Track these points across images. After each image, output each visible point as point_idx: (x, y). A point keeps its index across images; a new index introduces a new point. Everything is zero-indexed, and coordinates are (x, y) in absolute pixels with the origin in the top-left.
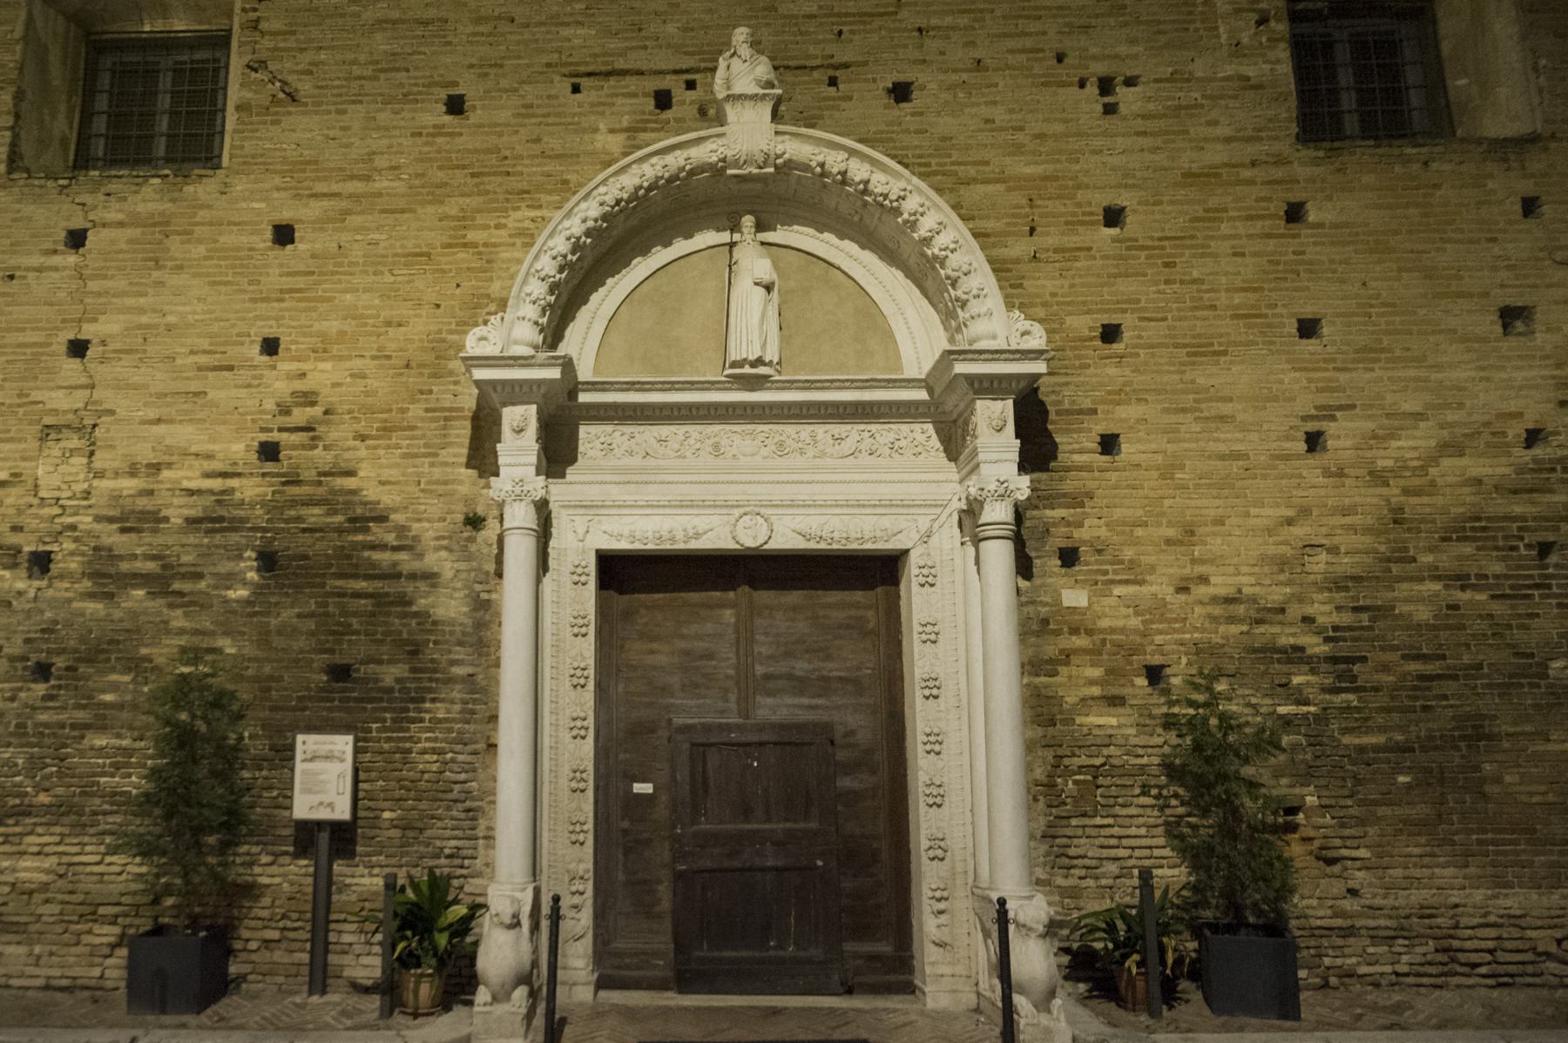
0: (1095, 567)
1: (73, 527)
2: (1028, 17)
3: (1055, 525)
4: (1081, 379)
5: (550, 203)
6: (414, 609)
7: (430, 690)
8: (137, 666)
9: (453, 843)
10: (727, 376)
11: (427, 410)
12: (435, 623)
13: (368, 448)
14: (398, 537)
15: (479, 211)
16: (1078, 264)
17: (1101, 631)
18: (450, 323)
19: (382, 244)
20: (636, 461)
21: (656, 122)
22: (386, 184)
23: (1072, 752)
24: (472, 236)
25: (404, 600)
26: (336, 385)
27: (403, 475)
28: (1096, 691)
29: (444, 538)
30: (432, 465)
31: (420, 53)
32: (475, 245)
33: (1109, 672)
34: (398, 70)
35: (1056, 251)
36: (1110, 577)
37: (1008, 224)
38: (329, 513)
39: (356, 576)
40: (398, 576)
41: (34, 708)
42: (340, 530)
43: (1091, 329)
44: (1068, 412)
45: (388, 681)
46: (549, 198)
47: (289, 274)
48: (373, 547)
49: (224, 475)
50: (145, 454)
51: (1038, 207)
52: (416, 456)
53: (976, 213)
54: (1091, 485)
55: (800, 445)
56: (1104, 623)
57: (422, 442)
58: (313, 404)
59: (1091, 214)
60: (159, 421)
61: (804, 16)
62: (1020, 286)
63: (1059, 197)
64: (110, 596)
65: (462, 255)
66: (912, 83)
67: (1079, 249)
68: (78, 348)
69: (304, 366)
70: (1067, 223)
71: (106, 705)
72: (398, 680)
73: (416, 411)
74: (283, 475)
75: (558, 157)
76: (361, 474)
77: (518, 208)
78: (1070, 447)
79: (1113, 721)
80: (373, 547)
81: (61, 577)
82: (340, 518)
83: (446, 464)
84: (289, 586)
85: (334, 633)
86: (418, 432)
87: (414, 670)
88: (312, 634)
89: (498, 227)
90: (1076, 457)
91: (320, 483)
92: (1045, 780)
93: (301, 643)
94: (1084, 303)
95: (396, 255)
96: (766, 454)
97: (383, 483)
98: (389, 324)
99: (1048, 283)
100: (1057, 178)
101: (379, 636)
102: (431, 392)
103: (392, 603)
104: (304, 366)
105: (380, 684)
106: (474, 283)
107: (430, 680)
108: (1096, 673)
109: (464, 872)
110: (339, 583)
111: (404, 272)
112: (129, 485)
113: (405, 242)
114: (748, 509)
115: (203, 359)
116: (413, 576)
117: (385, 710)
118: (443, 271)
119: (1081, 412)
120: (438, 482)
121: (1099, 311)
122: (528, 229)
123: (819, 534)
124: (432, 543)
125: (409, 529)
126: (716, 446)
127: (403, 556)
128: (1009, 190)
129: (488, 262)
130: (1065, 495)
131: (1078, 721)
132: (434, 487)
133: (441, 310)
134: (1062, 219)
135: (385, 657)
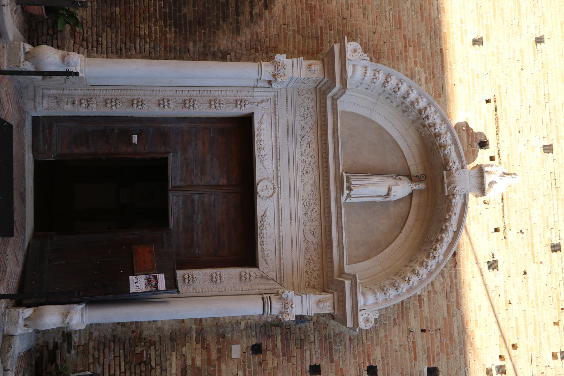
0: (252, 362)
2: (535, 328)
3: (273, 341)
4: (348, 355)
5: (429, 88)
6: (221, 22)
7: (181, 30)
9: (104, 42)
10: (342, 174)
12: (214, 32)
16: (407, 353)
17: (219, 365)
18: (365, 39)
19: (405, 5)
20: (299, 132)
21: (473, 141)
23: (158, 350)
24: (411, 49)
25: (225, 18)
27: (288, 16)
28: (189, 362)
29: (257, 37)
30: (294, 31)
31: (504, 22)
32: (406, 51)
33: (199, 369)
34: (495, 11)
35: (414, 342)
36: (247, 369)
37: (426, 318)
40: (238, 15)
43: (374, 360)
44: (331, 349)
45: (185, 10)
46: (431, 88)
51: (436, 334)
52: (298, 23)
53: (432, 302)
54: (294, 360)
55: (309, 213)
56: (223, 367)
57: (305, 25)
59: (434, 360)
61: (530, 214)
62: (395, 324)
63: (442, 345)
65: (400, 45)
66: (498, 270)
67: (415, 354)
70: (428, 348)
72: (185, 14)
77: (425, 72)
78: (313, 349)
79: (174, 371)
83: (294, 38)
86: (310, 24)
87: (190, 22)
89: (415, 62)
90: (308, 352)
92: (143, 337)
94: (387, 357)
95: (399, 11)
96: (304, 196)
98: (364, 9)
99: (397, 339)
100: (451, 343)
101: (207, 5)
102: (330, 30)
105: (183, 6)
106: (387, 51)
107: (186, 31)
108: (198, 363)
109: (90, 48)
111: (391, 16)
113: (406, 16)
114: (276, 187)
116: (238, 22)
117: (170, 8)
118: (392, 36)
119: (331, 355)
120: (285, 34)
121: (383, 364)
122: (415, 77)
123: (265, 223)
124: (254, 31)
125: (261, 19)
126: (308, 172)
127: (248, 17)
128: (445, 319)
129: (398, 58)
130: (288, 347)
131: (174, 354)
132: (283, 32)
133: (372, 35)
134: (430, 345)
135: (196, 8)
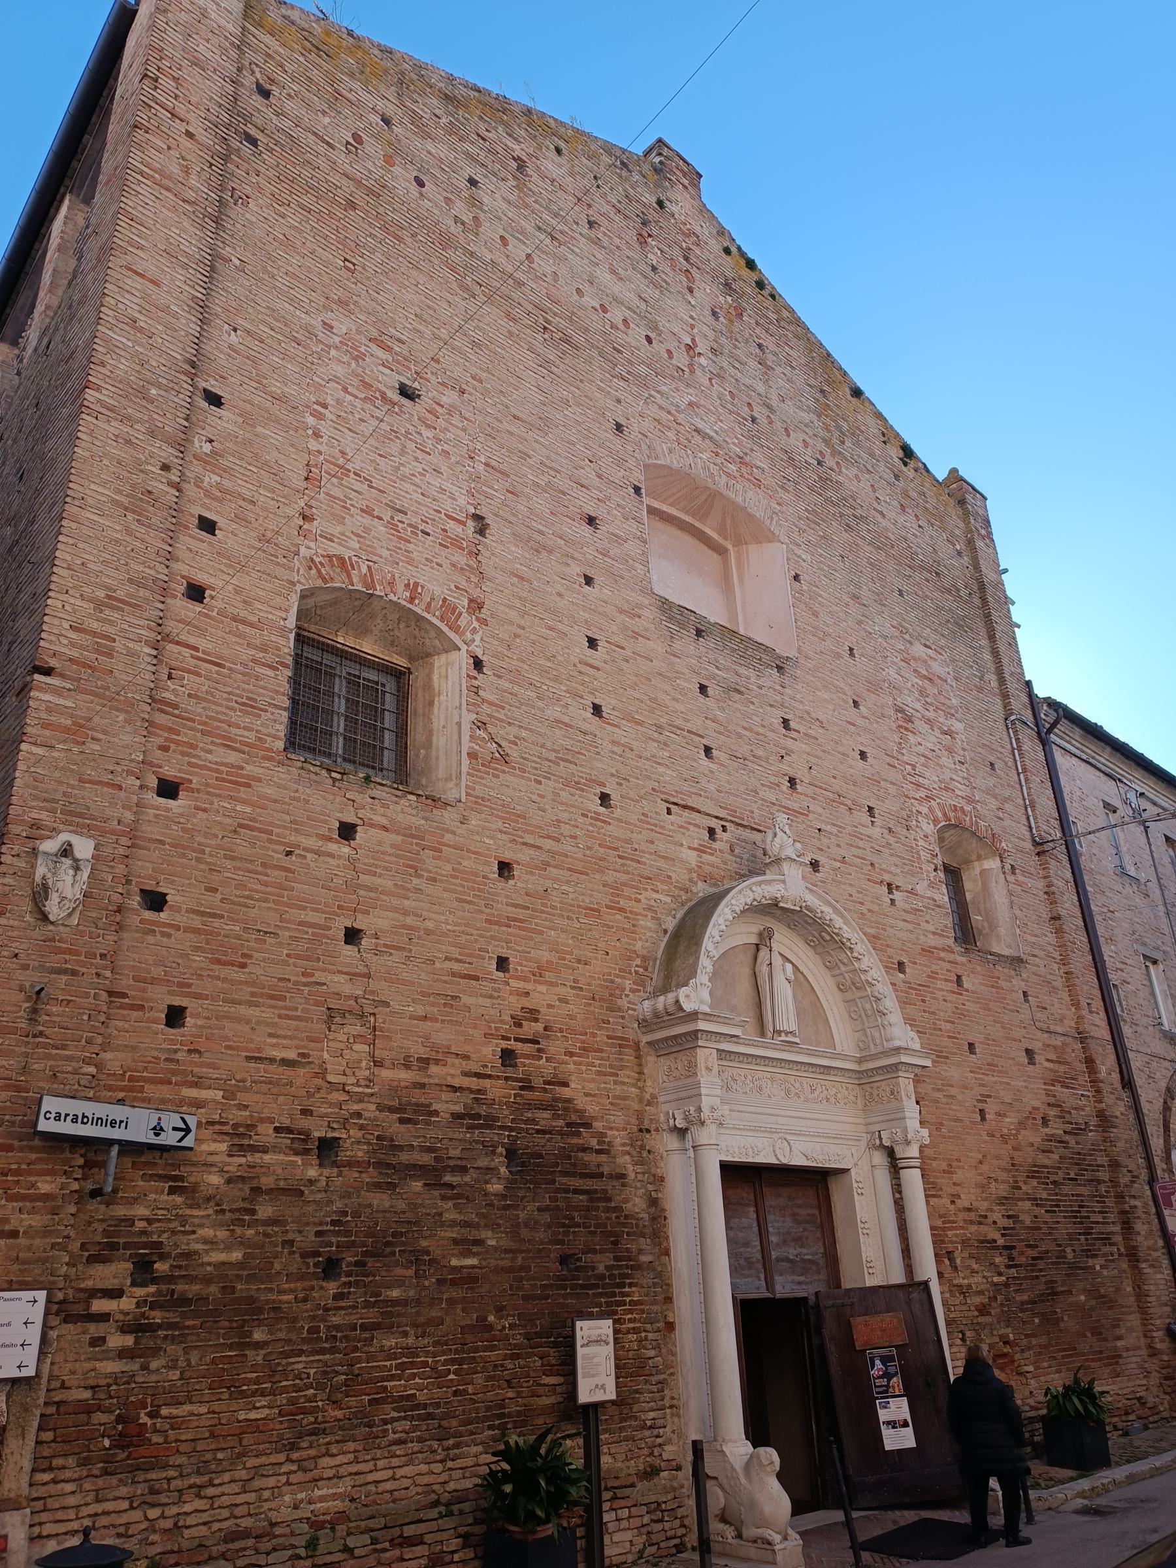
1: (358, 1115)
6: (613, 1204)
7: (627, 1276)
8: (419, 1259)
11: (609, 1037)
12: (626, 1217)
13: (575, 1063)
14: (599, 1143)
15: (625, 885)
22: (570, 848)
26: (550, 1006)
38: (556, 1117)
39: (574, 1174)
40: (601, 1175)
41: (326, 1310)
42: (561, 1133)
45: (601, 1268)
47: (513, 905)
48: (584, 1149)
49: (478, 1075)
50: (419, 1051)
58: (536, 1020)
60: (425, 1018)
64: (392, 1186)
65: (618, 917)
68: (352, 936)
69: (529, 986)
71: (395, 1302)
72: (608, 1268)
73: (601, 1036)
74: (520, 1080)
75: (664, 857)
76: (573, 1085)
80: (584, 1149)
81: (350, 1164)
82: (561, 1123)
83: (624, 1083)
84: (530, 1182)
85: (564, 1225)
86: (604, 1055)
87: (616, 1259)
88: (549, 1226)
91: (545, 1091)
93: (541, 1235)
95: (579, 906)
97: (587, 1095)
102: (609, 1022)
103: (599, 1200)
104: (529, 986)
107: (627, 1267)
110: (565, 1180)
112: (404, 1076)
115: (456, 966)
117: (601, 1295)
120: (618, 1097)
127: (603, 1158)
129: (634, 926)
